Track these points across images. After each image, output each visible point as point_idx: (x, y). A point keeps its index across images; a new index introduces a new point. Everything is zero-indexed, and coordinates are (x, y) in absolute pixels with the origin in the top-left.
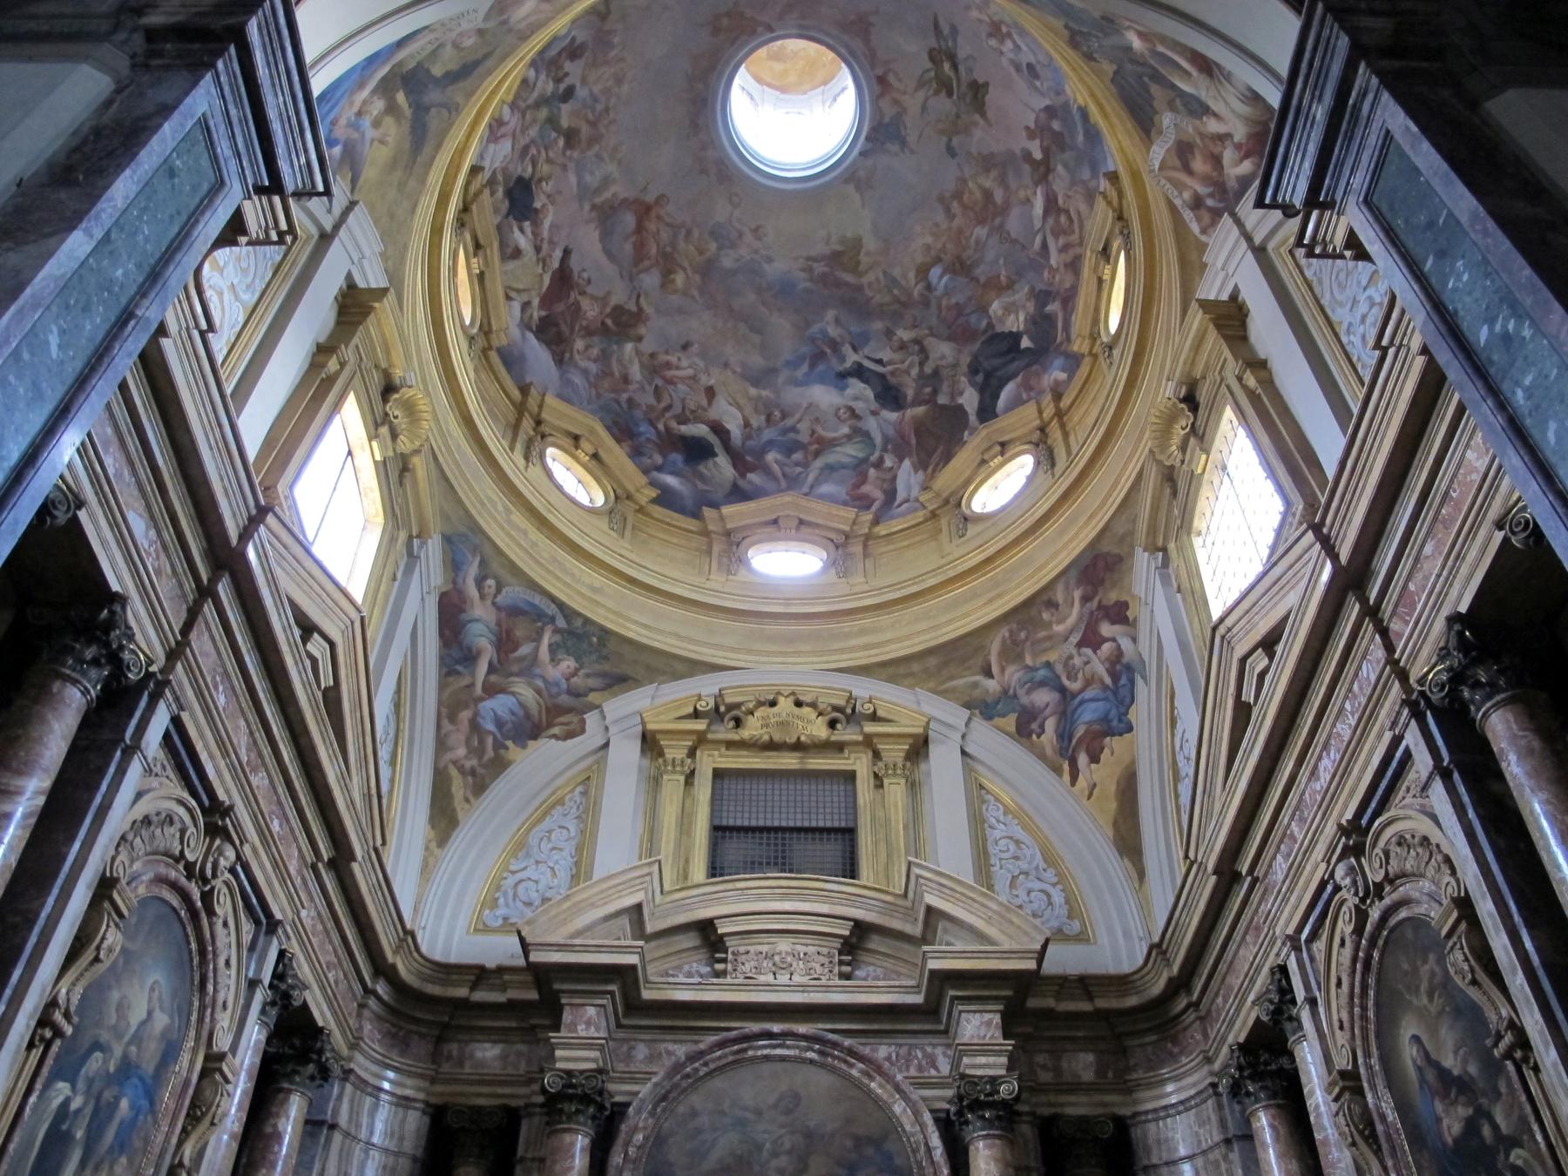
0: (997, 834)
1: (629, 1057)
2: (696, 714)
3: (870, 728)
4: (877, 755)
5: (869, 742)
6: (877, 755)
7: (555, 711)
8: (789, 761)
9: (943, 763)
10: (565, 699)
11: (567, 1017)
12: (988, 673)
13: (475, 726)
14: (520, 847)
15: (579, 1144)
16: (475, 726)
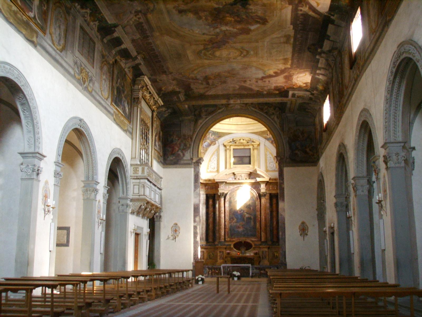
0: (268, 156)
1: (226, 188)
2: (230, 142)
3: (253, 143)
4: (253, 146)
5: (253, 145)
6: (253, 146)
7: (212, 142)
8: (242, 147)
9: (262, 147)
10: (213, 140)
11: (220, 186)
12: (268, 135)
13: (203, 147)
14: (210, 160)
15: (222, 199)
16: (203, 147)
